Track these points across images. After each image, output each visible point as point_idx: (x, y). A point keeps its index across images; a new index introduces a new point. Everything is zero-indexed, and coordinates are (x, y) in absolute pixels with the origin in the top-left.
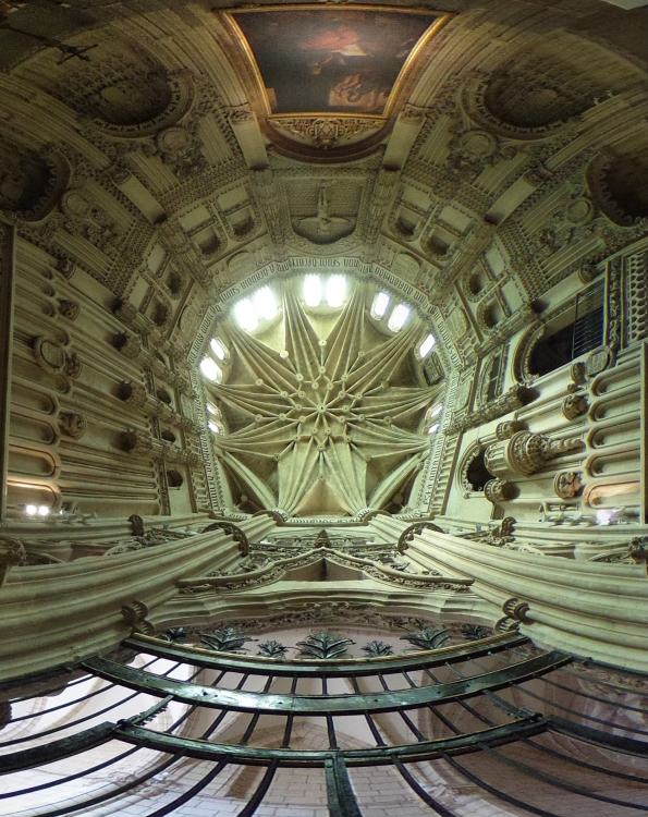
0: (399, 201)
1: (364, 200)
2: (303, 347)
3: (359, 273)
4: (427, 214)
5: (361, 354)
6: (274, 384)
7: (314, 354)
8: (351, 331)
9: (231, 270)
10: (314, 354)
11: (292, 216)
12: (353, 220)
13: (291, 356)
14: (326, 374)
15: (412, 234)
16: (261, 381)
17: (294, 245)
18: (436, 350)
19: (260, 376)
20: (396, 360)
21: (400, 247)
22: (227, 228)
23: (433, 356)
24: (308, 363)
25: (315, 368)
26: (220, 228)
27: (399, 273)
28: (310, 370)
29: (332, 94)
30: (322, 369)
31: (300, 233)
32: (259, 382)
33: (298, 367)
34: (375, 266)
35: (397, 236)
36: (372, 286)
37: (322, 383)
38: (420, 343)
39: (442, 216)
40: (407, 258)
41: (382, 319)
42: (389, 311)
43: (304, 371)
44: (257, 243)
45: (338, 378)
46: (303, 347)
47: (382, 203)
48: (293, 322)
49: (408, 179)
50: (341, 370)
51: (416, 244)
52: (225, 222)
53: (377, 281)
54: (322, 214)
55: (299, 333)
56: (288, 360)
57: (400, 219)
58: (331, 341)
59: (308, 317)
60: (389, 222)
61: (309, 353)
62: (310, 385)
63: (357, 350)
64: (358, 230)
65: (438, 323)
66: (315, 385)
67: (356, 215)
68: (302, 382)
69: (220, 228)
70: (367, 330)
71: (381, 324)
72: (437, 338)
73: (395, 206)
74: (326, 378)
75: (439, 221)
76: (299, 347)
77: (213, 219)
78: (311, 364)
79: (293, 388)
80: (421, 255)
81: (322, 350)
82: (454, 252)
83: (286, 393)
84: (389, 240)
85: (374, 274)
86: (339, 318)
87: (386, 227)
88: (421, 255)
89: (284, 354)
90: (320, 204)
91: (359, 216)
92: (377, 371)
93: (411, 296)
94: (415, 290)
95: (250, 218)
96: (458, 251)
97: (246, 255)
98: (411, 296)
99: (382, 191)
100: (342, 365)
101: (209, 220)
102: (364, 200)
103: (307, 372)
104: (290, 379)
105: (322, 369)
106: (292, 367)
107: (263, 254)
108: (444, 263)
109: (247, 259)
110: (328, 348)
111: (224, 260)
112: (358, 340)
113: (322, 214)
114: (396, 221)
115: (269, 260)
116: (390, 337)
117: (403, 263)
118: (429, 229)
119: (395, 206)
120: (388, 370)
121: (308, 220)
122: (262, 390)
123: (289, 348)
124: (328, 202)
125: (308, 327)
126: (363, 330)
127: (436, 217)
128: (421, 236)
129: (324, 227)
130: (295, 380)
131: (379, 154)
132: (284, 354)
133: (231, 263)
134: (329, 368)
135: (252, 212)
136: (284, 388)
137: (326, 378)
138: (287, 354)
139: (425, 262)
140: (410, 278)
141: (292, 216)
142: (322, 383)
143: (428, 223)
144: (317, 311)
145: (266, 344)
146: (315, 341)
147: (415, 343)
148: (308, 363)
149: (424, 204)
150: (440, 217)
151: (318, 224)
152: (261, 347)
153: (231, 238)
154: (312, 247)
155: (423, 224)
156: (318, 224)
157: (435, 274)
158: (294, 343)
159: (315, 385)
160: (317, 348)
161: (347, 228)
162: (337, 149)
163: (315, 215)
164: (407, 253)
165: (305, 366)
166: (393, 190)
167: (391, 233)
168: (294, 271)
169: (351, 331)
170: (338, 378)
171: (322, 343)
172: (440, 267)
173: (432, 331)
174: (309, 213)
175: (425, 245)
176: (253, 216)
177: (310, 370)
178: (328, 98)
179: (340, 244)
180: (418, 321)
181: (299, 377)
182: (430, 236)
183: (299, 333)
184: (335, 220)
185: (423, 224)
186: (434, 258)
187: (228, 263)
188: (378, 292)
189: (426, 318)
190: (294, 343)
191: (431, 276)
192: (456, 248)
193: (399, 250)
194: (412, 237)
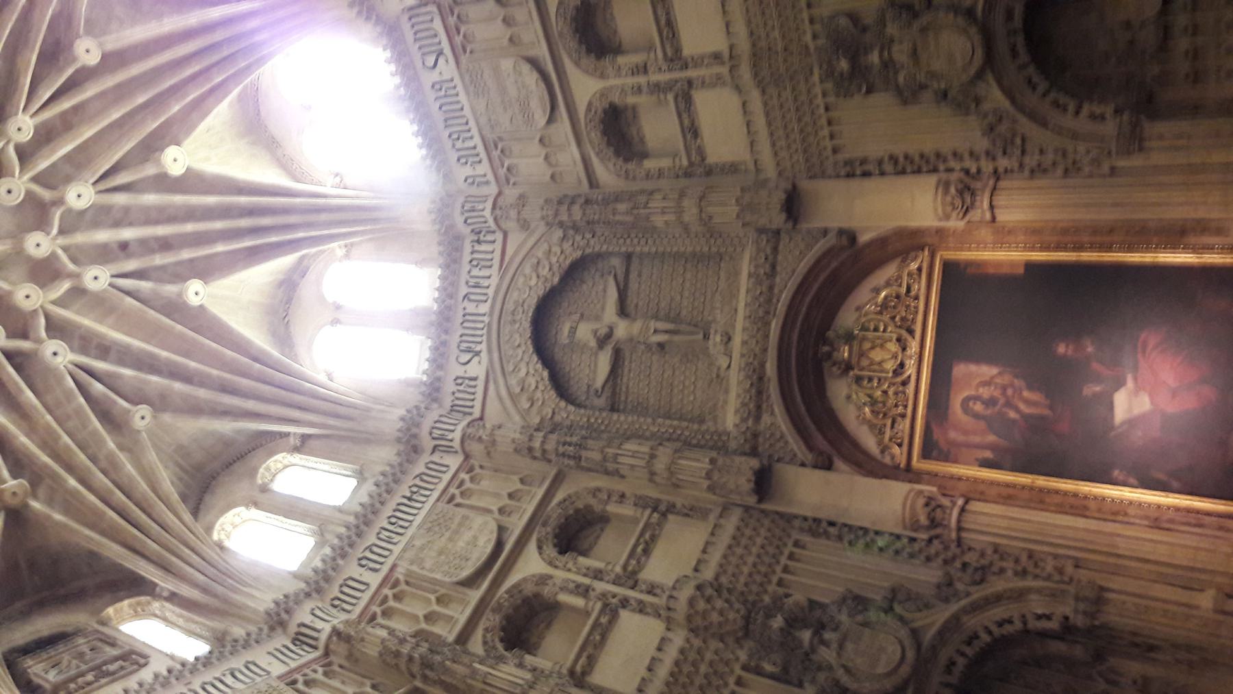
0: (664, 511)
1: (664, 426)
2: (189, 227)
3: (433, 415)
4: (630, 578)
5: (141, 417)
6: (66, 104)
7: (159, 260)
8: (225, 389)
9: (507, 64)
10: (159, 260)
11: (628, 257)
12: (601, 402)
13: (163, 182)
14: (78, 292)
15: (562, 552)
16: (93, 59)
17: (540, 254)
18: (158, 666)
19: (111, 61)
20: (95, 522)
21: (517, 524)
22: (638, 90)
23: (134, 657)
24: (128, 234)
25: (103, 254)
26: (644, 69)
27: (434, 525)
28: (103, 236)
29: (988, 371)
30: (97, 278)
31: (574, 273)
32: (87, 52)
33: (121, 199)
34: (454, 462)
36: (384, 456)
37: (44, 272)
38: (170, 609)
40: (485, 546)
41: (264, 489)
42: (292, 509)
43: (99, 216)
44: (570, 157)
45: (56, 328)
46: (189, 227)
47: (660, 465)
48: (286, 211)
49: (732, 522)
50: (85, 342)
51: (532, 564)
52: (656, 88)
53: (392, 479)
54: (622, 329)
55: (244, 223)
56: (150, 170)
57: (604, 519)
58: (199, 320)
59: (285, 262)
60: (595, 492)
61: (165, 245)
62: (41, 224)
63: (160, 403)
64: (567, 413)
65: (264, 660)
66: (39, 244)
67: (613, 409)
68: (60, 202)
69: (644, 69)
70: (226, 442)
71: (242, 488)
72: (205, 662)
73: (642, 502)
74: (66, 285)
75: (611, 610)
76: (191, 214)
77: (676, 58)
78: (124, 246)
79: (43, 165)
80: (496, 583)
81: (170, 289)
82: (521, 665)
83: (26, 136)
84: (540, 493)
85: (426, 458)
86: (276, 353)
87: (578, 486)
88: (496, 583)
89: (175, 160)
90: (661, 325)
91: (615, 416)
92: (70, 468)
93: (354, 570)
94: (374, 580)
95: (644, 155)
96: (528, 676)
97: (541, 119)
98: (354, 570)
99: (695, 465)
100: (104, 350)
101: (678, 50)
102: (664, 426)
103: (96, 224)
104: (78, 162)
105: (97, 278)
106: (122, 179)
107: (531, 164)
108: (476, 645)
109: (529, 119)
110: (176, 309)
111: (542, 52)
112: (196, 409)
113: (622, 329)
114: (598, 508)
115: (506, 177)
116: (195, 513)
117: (467, 536)
118: (584, 591)
119: (642, 502)
120: (71, 505)
121: (613, 294)
122: (54, 54)
123: (192, 182)
124: (661, 346)
125: (254, 255)
126: (226, 426)
127: (625, 603)
128: (560, 575)
129: (585, 332)
130: (68, 180)
132: (175, 160)
133: (526, 68)
134: (99, 304)
135: (665, 163)
136: (46, 136)
137: (66, 285)
138: (176, 170)
139: (475, 595)
140: (419, 561)
141: (628, 257)
142: (44, 272)
143: (601, 586)
144: (306, 290)
145: (222, 113)
146: (206, 270)
147: (173, 598)
148: (128, 234)
150: (624, 614)
151: (598, 318)
152: (217, 92)
153: (603, 94)
154: (530, 291)
155: (598, 575)
156: (598, 318)
157: (438, 629)
158: (211, 200)
159: (39, 244)
160: (181, 273)
161: (578, 388)
163: (623, 311)
164: (499, 545)
165: (117, 224)
167: (560, 496)
168: (459, 238)
169: (225, 389)
170: (56, 328)
171: (195, 292)
172: (463, 638)
173: (222, 645)
174: (632, 299)
175: (529, 589)
176: (649, 164)
177: (103, 236)
178: (978, 360)
179: (531, 370)
180: (263, 601)
181: (80, 195)
182: (563, 598)
183: (244, 223)
184: (604, 363)
185: (598, 575)
186: (491, 620)
187: (534, 63)
188: (361, 475)
189: (277, 620)
190: (211, 200)
191: (429, 618)
192: (534, 670)
193: (506, 520)
194: (551, 551)
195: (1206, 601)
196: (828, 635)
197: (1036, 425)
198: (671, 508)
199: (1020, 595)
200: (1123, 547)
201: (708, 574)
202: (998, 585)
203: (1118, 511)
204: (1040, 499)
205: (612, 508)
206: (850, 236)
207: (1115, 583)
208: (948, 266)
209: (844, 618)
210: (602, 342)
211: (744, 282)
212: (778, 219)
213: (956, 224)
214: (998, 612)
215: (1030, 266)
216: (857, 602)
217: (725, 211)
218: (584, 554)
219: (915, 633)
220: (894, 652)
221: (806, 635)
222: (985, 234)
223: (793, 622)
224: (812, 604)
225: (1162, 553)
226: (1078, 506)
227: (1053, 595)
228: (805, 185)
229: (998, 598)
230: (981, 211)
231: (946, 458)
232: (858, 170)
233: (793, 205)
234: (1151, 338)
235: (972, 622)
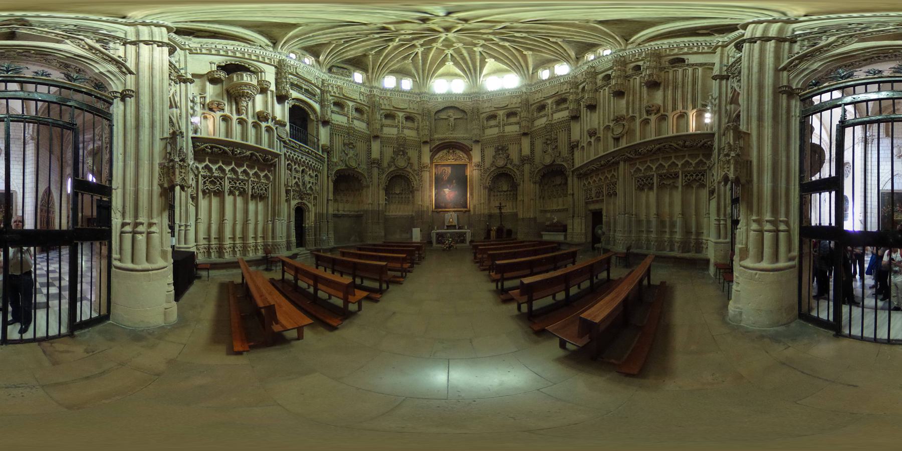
0: (417, 129)
1: (433, 127)
4: (403, 128)
12: (436, 117)
29: (450, 171)
35: (412, 115)
39: (396, 129)
49: (417, 139)
57: (414, 122)
64: (433, 114)
67: (435, 120)
87: (420, 118)
99: (426, 132)
102: (433, 127)
113: (452, 119)
121: (459, 117)
131: (432, 148)
149: (406, 132)
155: (402, 123)
162: (447, 148)
163: (455, 119)
166: (421, 133)
174: (458, 120)
178: (451, 171)
195: (420, 203)
196: (402, 156)
197: (442, 179)
198: (418, 131)
199: (416, 180)
200: (425, 192)
201: (407, 138)
202: (417, 177)
203: (431, 191)
204: (431, 181)
205: (416, 123)
206: (471, 150)
207: (420, 192)
208: (466, 165)
209: (406, 157)
210: (449, 116)
211: (462, 136)
212: (474, 139)
213: (473, 165)
214: (413, 178)
215: (467, 176)
216: (409, 159)
217: (475, 132)
218: (406, 121)
219: (406, 168)
220: (403, 165)
221: (401, 153)
222: (472, 169)
223: (403, 151)
224: (407, 153)
225: (425, 197)
226: (431, 186)
227: (417, 185)
228: (480, 143)
229: (415, 178)
230: (475, 168)
231: (435, 168)
232: (482, 151)
233: (477, 142)
234: (457, 193)
235: (410, 175)
